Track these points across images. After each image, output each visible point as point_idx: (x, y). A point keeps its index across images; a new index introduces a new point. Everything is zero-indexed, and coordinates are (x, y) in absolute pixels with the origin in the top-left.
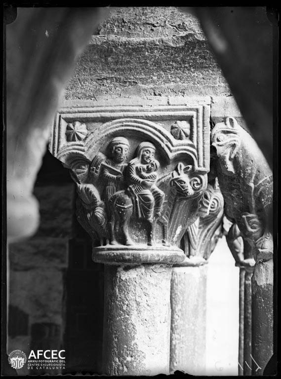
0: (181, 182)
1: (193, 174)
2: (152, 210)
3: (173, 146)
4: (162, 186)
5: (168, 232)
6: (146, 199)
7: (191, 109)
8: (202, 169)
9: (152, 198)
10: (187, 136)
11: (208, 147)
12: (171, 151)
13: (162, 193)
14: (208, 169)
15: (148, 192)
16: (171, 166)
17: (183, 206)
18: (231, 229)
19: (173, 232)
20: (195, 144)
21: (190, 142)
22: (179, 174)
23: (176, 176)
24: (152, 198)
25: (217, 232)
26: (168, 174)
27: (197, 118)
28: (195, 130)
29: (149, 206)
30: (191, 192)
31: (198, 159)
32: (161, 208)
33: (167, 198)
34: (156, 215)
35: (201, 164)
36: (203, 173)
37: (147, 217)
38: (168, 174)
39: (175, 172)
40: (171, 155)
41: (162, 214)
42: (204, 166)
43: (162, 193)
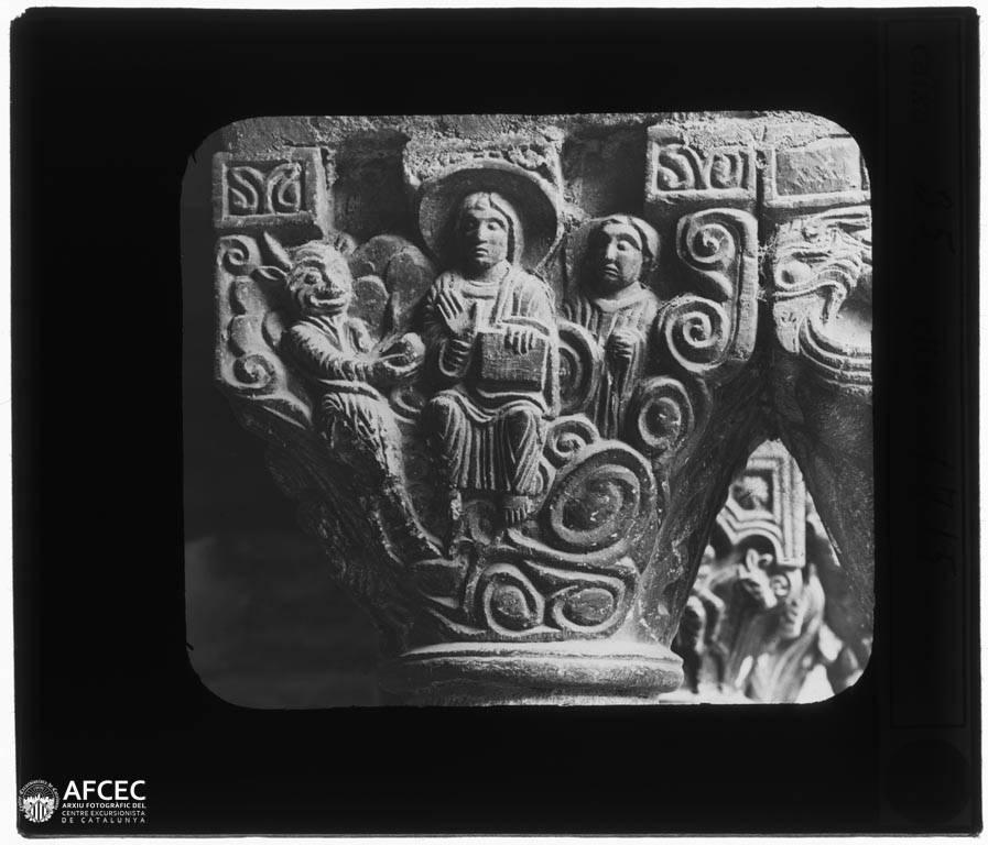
0: (754, 584)
1: (774, 570)
2: (701, 632)
3: (737, 520)
4: (719, 590)
5: (728, 674)
6: (691, 614)
7: (772, 458)
8: (791, 562)
9: (701, 612)
10: (762, 503)
11: (802, 527)
12: (735, 530)
13: (719, 603)
14: (801, 561)
15: (694, 603)
16: (734, 556)
17: (755, 623)
18: (840, 655)
19: (736, 670)
20: (778, 520)
21: (768, 515)
22: (748, 570)
23: (744, 575)
24: (701, 612)
25: (807, 662)
26: (729, 572)
27: (780, 472)
28: (776, 494)
29: (697, 626)
30: (771, 602)
31: (783, 544)
32: (718, 628)
33: (730, 611)
34: (708, 641)
35: (789, 554)
36: (792, 569)
37: (693, 644)
38: (729, 572)
39: (741, 568)
40: (735, 538)
41: (720, 638)
42: (794, 556)
43: (719, 603)
